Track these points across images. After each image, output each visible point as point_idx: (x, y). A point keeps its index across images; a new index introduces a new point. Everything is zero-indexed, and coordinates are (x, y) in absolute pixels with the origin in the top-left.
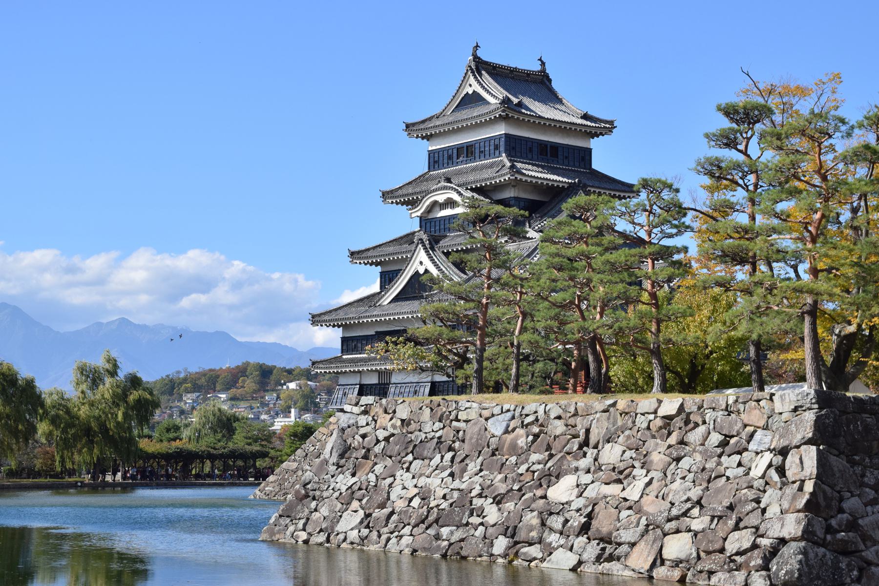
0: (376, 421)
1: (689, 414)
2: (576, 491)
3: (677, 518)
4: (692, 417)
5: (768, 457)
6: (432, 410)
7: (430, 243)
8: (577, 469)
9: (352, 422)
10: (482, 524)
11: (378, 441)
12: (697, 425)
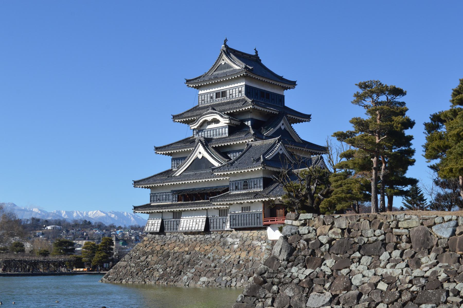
0: (316, 230)
6: (370, 222)
7: (205, 142)
9: (293, 231)
11: (322, 244)
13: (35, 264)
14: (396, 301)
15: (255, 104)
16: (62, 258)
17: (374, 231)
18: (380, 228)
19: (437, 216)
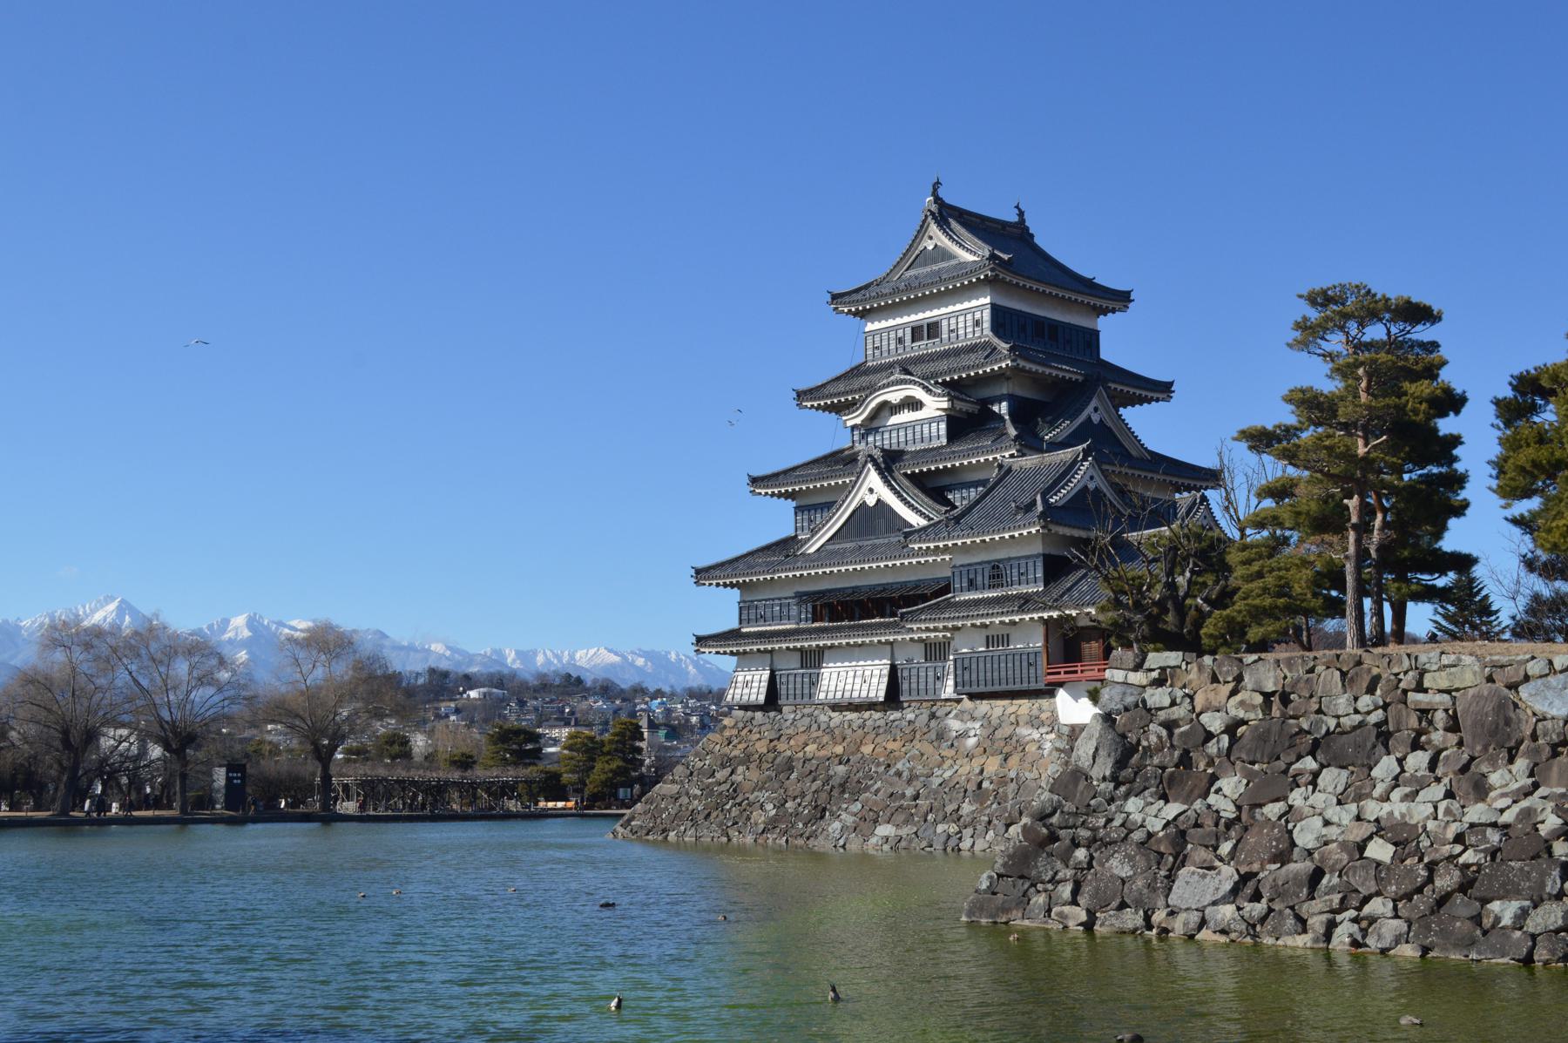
0: (1191, 698)
6: (1343, 674)
9: (1130, 700)
11: (1209, 736)
13: (438, 791)
14: (1419, 890)
15: (1020, 356)
16: (510, 775)
17: (1356, 699)
18: (1371, 690)
19: (1533, 658)
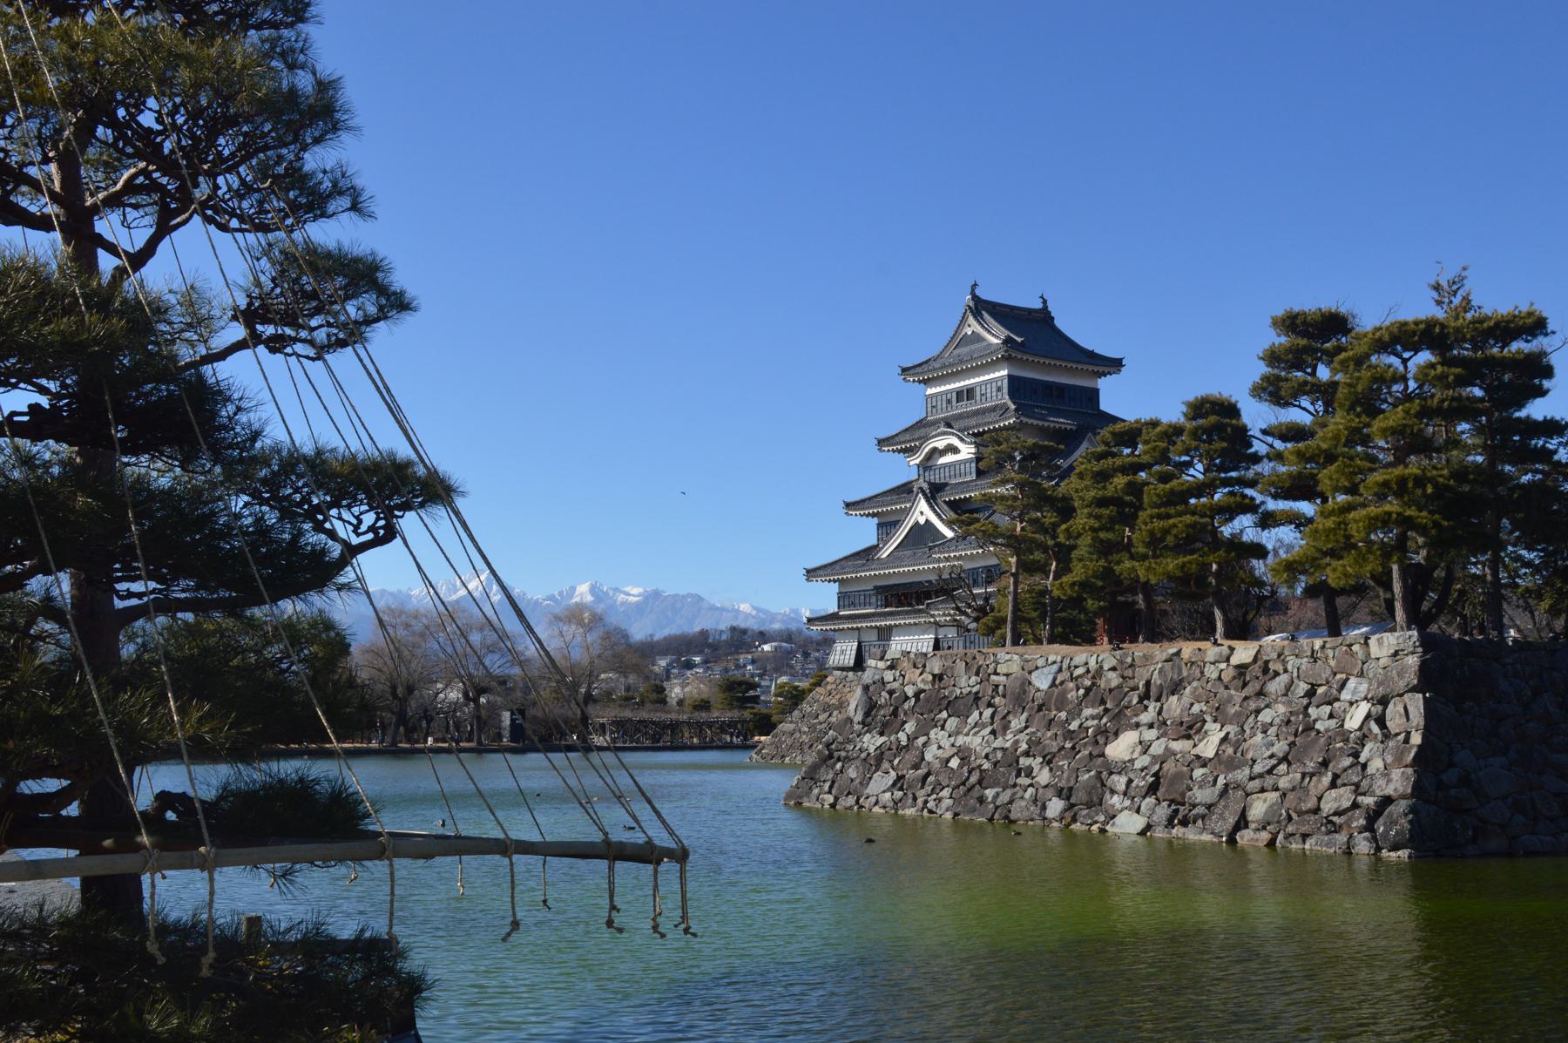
1: (1267, 662)
2: (1139, 748)
3: (1261, 776)
4: (1272, 666)
5: (1364, 708)
8: (1138, 725)
10: (1031, 785)
11: (907, 698)
12: (1277, 674)
13: (674, 727)
16: (735, 714)
